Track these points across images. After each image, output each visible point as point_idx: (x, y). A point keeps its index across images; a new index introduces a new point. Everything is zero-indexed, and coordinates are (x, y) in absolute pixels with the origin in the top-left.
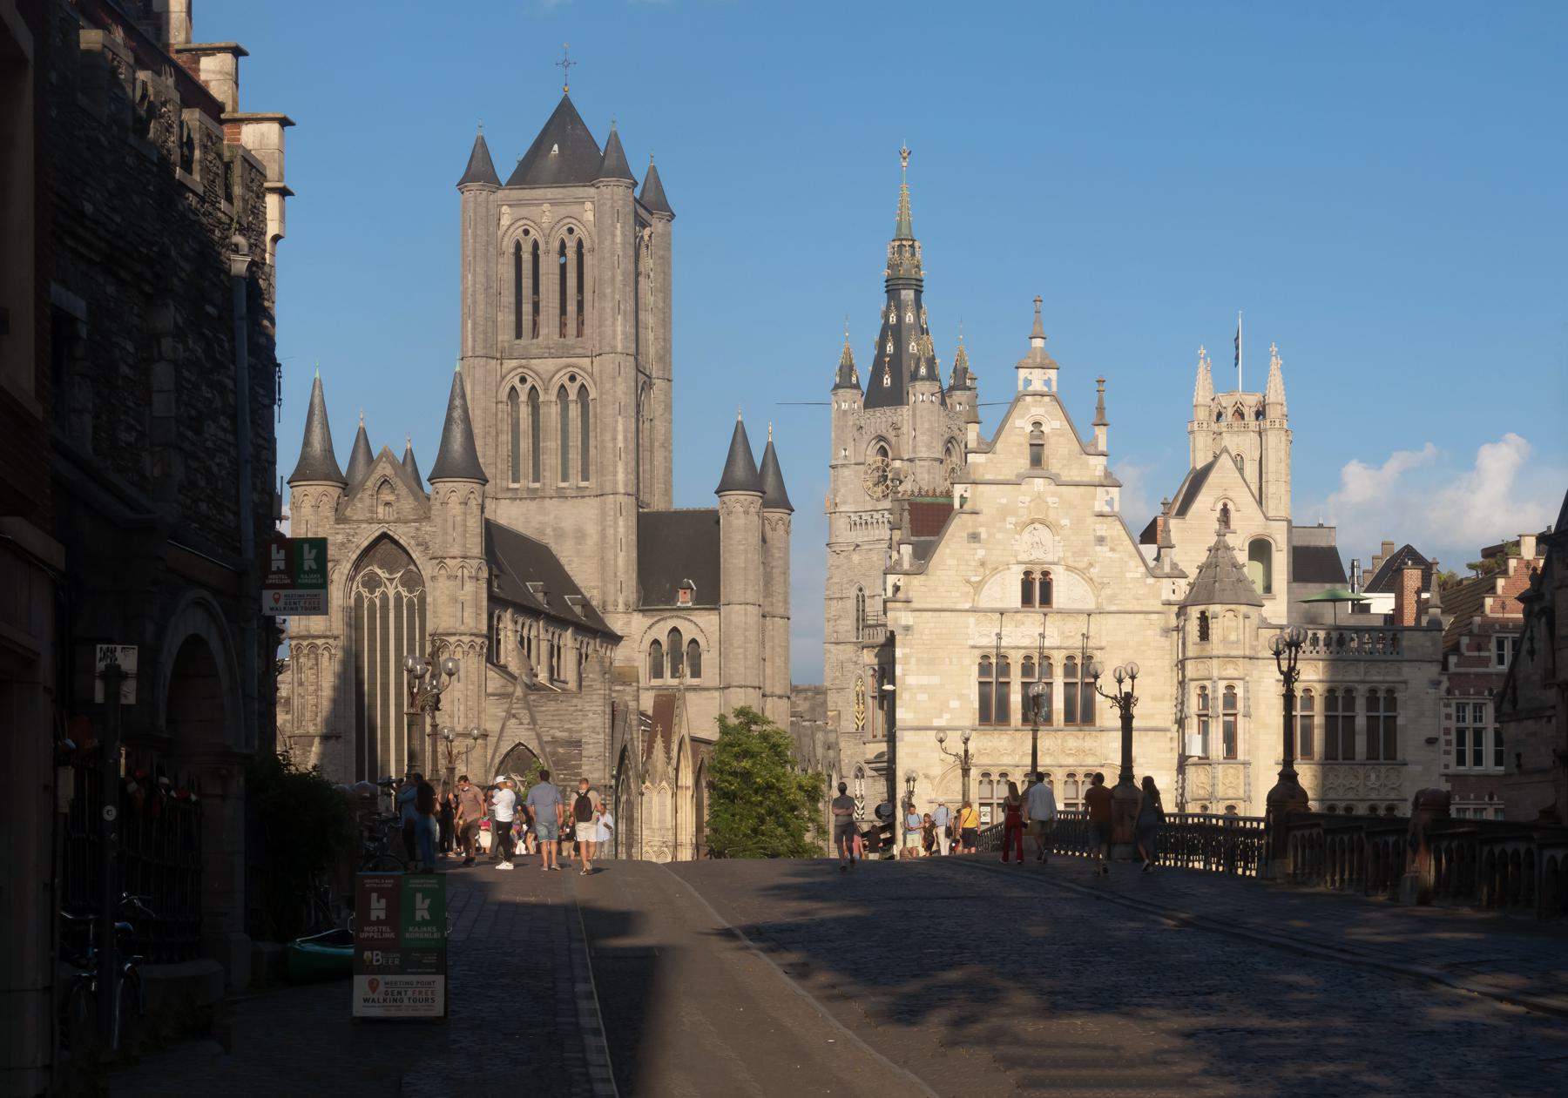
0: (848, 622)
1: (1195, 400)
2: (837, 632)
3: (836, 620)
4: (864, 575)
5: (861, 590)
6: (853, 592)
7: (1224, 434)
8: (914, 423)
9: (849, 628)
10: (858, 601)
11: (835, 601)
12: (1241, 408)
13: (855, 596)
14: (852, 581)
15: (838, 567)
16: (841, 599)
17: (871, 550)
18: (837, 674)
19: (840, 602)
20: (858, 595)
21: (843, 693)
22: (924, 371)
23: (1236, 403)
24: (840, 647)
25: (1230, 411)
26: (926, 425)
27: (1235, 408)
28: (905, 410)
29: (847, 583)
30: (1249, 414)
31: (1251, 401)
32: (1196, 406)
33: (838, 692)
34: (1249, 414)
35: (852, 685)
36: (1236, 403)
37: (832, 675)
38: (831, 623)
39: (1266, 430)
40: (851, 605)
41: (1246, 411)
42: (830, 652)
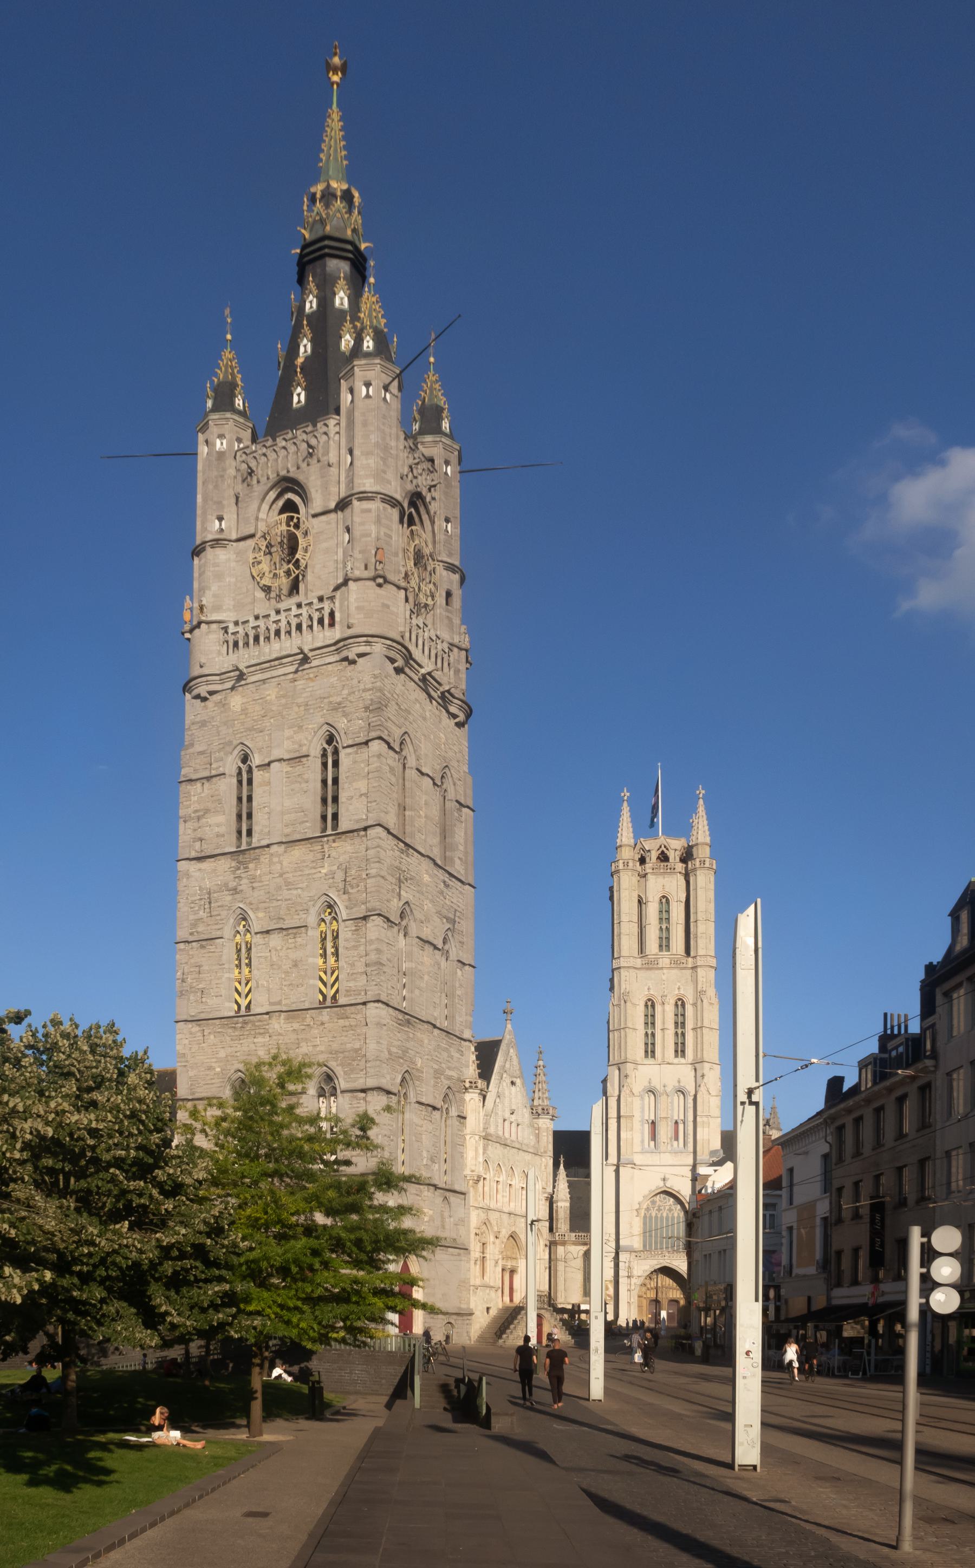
0: (221, 819)
1: (618, 841)
2: (201, 840)
3: (199, 818)
4: (251, 729)
5: (245, 759)
6: (231, 764)
7: (649, 876)
8: (351, 438)
9: (222, 830)
10: (240, 782)
11: (199, 784)
12: (666, 851)
13: (234, 771)
14: (230, 742)
15: (203, 724)
16: (208, 778)
17: (264, 681)
18: (201, 913)
19: (207, 785)
20: (240, 768)
21: (212, 948)
22: (371, 344)
23: (661, 847)
24: (207, 865)
25: (654, 855)
26: (374, 438)
27: (660, 852)
28: (332, 422)
29: (219, 751)
30: (674, 856)
31: (676, 845)
32: (621, 846)
33: (202, 947)
34: (674, 856)
35: (228, 932)
36: (661, 847)
37: (192, 917)
38: (189, 824)
39: (695, 870)
40: (227, 787)
41: (671, 854)
42: (188, 875)
